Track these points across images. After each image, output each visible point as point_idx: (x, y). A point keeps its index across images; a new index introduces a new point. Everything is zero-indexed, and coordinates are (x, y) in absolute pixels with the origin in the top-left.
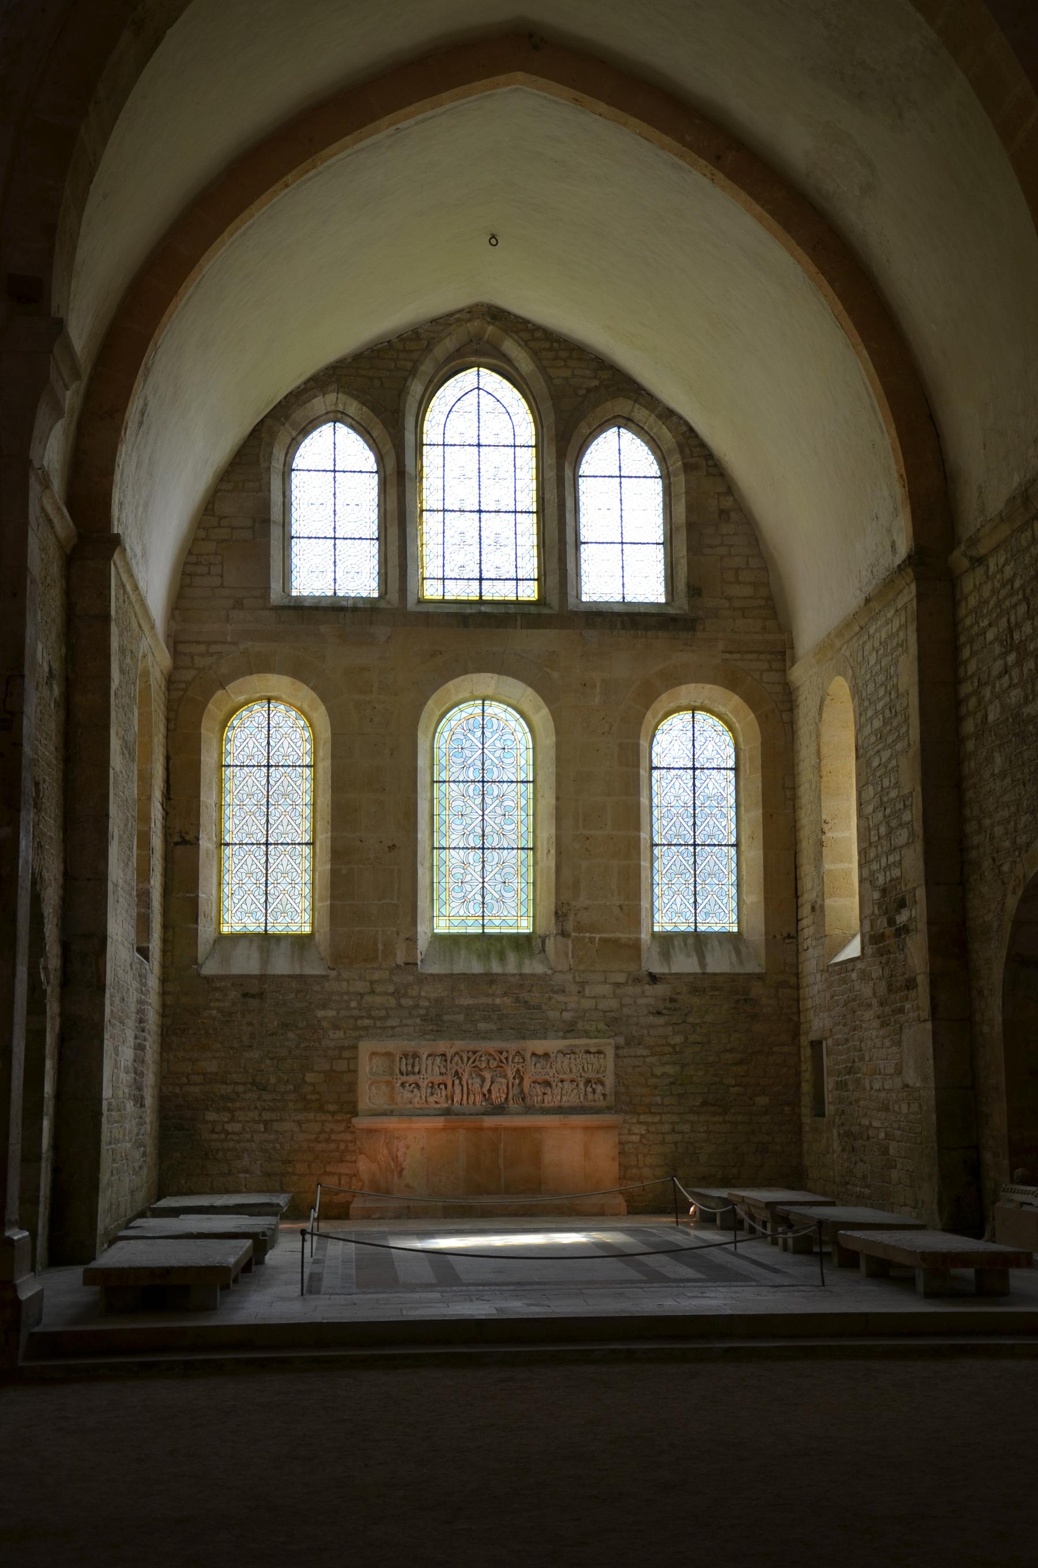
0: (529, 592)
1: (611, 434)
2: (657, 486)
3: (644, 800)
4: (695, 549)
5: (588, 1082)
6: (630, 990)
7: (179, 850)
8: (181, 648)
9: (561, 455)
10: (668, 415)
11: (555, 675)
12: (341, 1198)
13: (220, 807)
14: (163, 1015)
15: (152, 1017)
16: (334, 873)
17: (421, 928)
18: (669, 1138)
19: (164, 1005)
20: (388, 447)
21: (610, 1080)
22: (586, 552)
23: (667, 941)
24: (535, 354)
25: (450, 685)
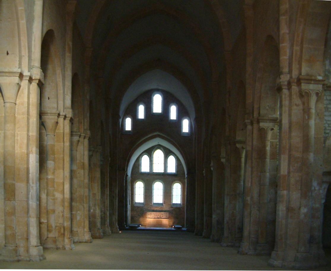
0: (163, 171)
9: (166, 159)
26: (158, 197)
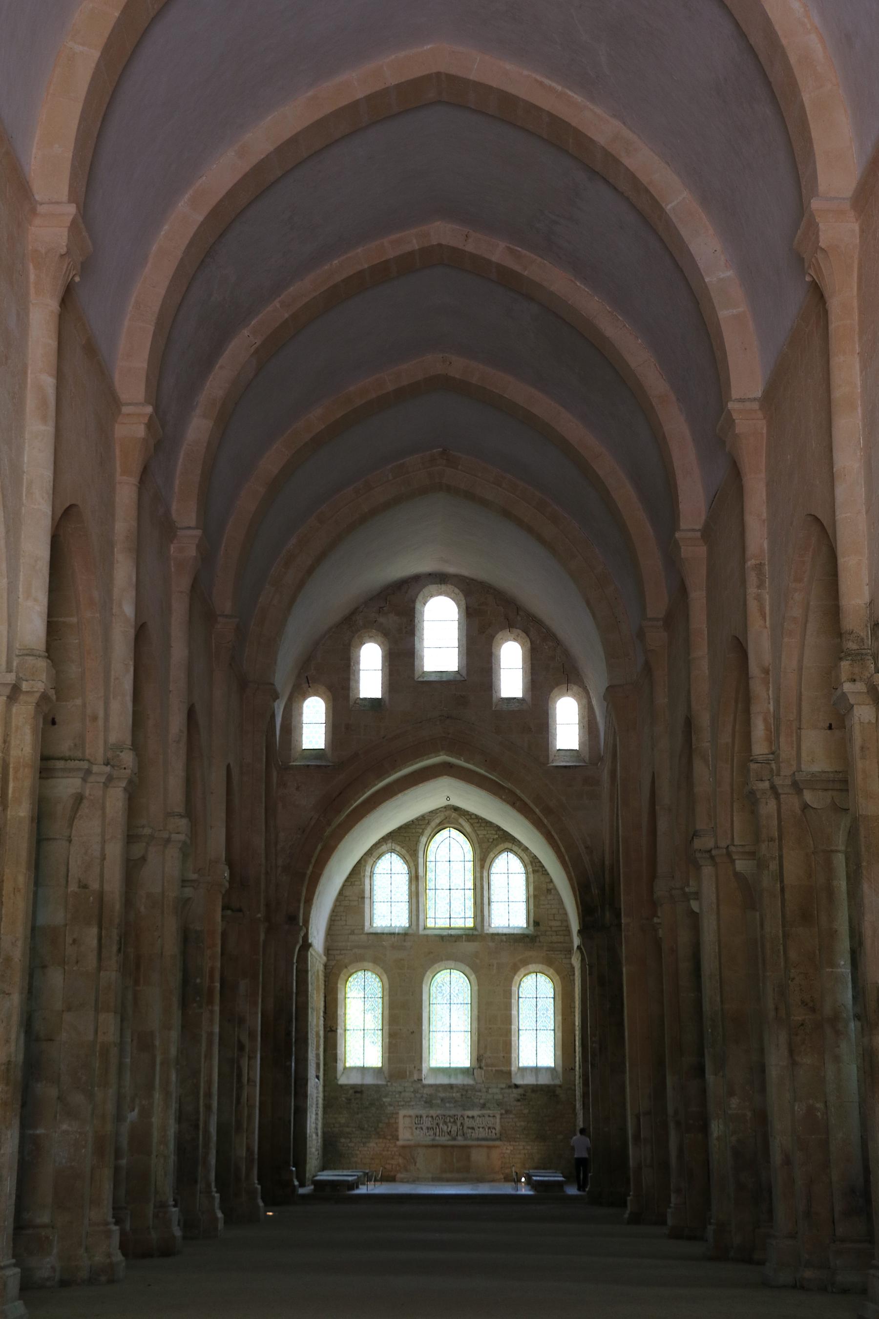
0: (470, 923)
1: (504, 855)
2: (523, 877)
3: (514, 1012)
4: (537, 906)
5: (489, 1128)
6: (507, 1091)
7: (330, 1034)
8: (330, 952)
9: (482, 867)
10: (526, 849)
11: (478, 961)
12: (392, 1174)
13: (345, 1014)
14: (324, 1100)
15: (321, 1101)
16: (390, 1043)
17: (424, 1065)
18: (523, 1152)
19: (324, 1096)
20: (412, 865)
21: (498, 1127)
22: (494, 906)
23: (525, 1069)
24: (472, 824)
25: (436, 966)
26: (449, 1045)
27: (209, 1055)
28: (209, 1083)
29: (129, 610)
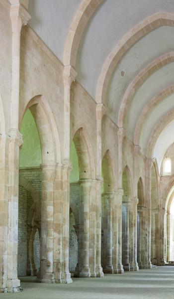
27: (135, 236)
28: (135, 242)
29: (100, 147)
